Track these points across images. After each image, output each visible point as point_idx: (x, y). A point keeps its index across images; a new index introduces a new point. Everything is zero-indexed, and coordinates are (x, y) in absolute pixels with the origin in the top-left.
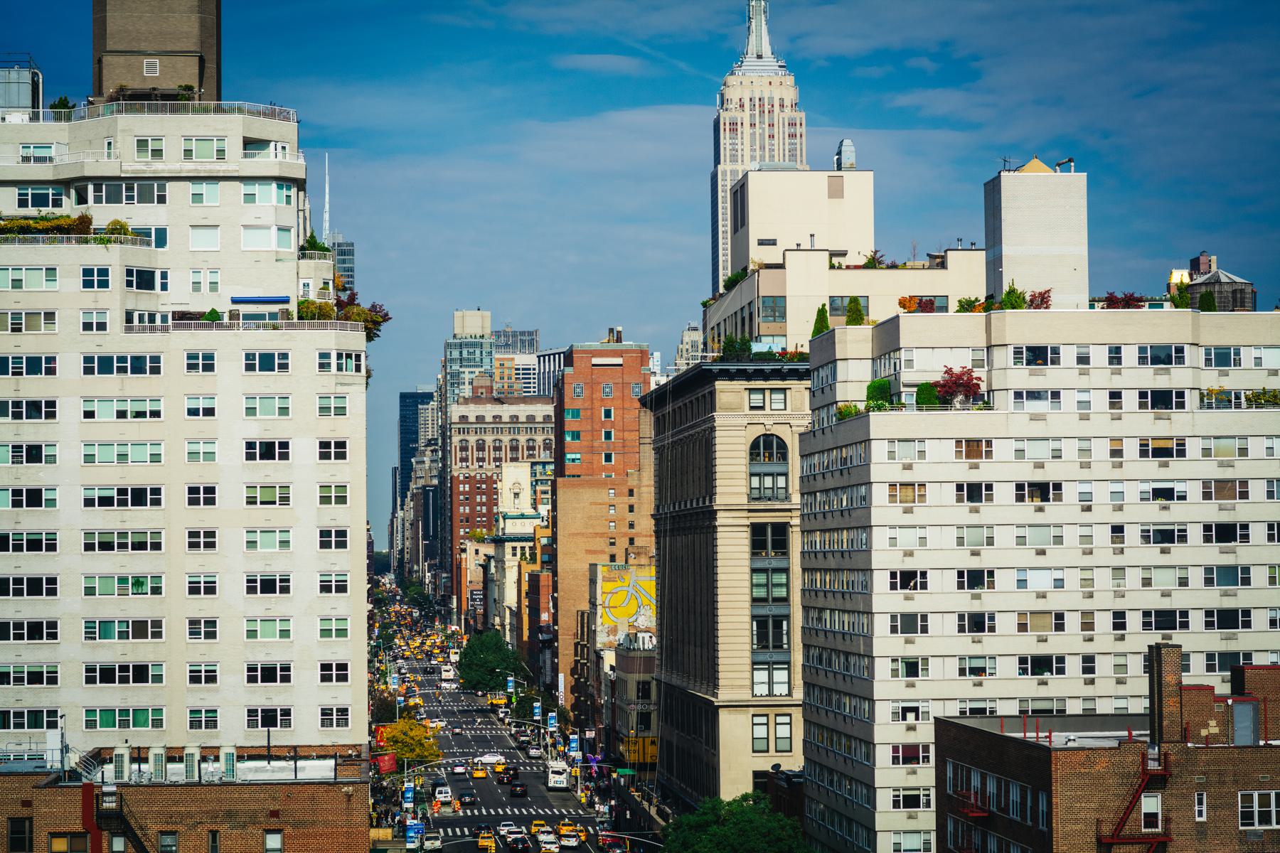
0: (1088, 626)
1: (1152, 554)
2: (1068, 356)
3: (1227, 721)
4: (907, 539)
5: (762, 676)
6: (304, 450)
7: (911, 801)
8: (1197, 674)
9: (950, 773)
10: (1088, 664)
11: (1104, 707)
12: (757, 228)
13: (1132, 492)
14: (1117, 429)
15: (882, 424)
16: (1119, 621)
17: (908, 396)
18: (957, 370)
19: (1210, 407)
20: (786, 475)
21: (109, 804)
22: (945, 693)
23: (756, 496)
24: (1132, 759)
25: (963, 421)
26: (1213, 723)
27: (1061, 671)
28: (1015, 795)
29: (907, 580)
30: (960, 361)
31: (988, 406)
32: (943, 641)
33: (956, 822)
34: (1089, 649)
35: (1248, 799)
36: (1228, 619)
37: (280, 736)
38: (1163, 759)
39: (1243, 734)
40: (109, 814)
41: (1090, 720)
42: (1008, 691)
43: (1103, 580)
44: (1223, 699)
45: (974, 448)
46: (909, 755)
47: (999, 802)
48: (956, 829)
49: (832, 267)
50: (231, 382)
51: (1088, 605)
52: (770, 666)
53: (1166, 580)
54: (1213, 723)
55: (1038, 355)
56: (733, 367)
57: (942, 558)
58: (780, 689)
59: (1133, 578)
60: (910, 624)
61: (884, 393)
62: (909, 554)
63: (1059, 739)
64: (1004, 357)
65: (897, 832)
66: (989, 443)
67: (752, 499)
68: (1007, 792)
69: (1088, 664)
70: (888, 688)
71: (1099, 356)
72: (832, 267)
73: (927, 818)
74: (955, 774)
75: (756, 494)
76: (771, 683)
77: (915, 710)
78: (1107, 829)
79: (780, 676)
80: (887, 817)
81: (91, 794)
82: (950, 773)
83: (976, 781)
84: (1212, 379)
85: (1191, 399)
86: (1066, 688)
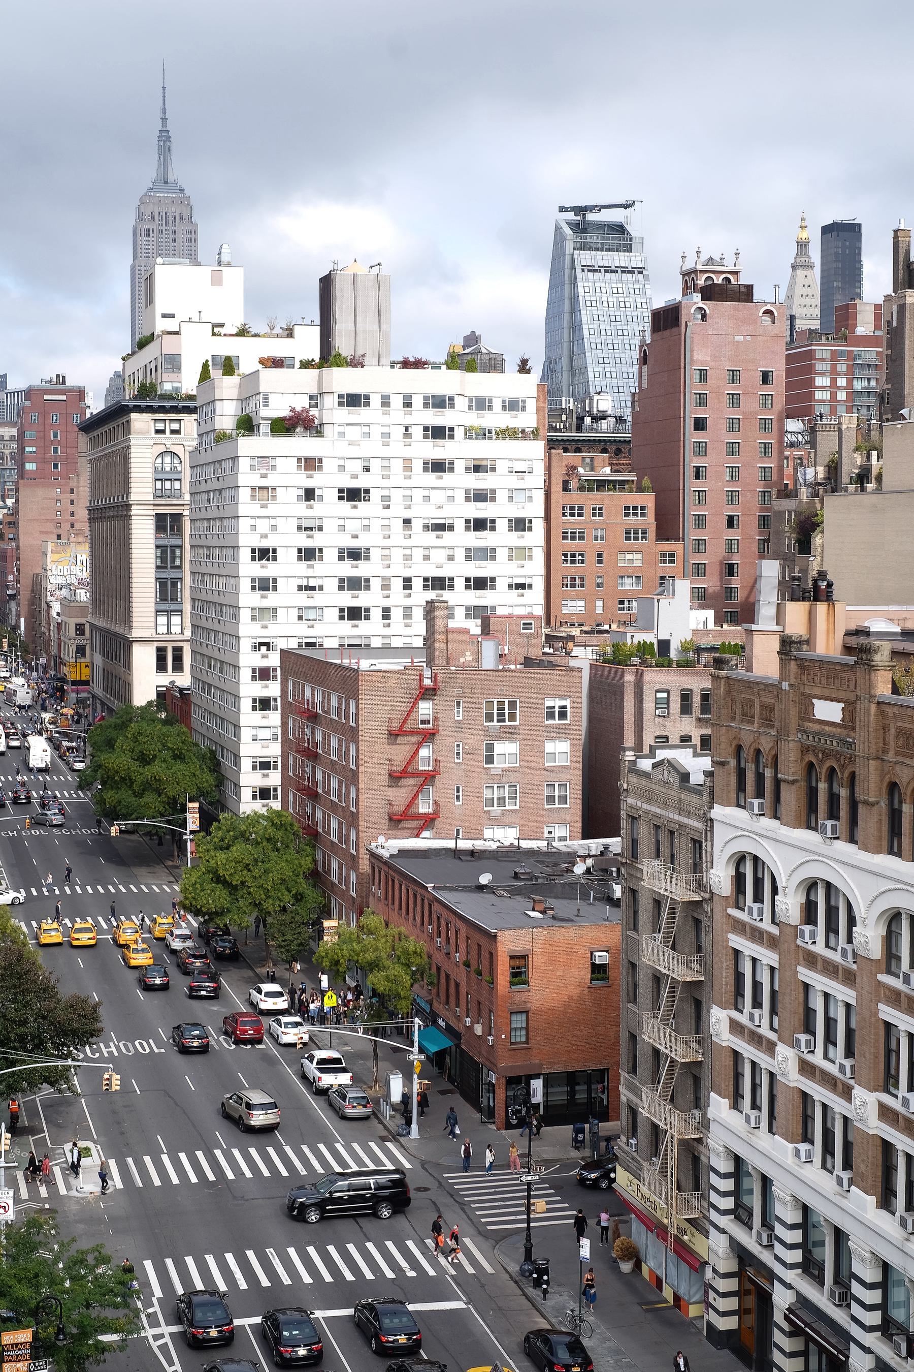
0: (386, 587)
1: (431, 538)
2: (376, 401)
3: (478, 653)
4: (263, 526)
5: (162, 620)
7: (264, 704)
8: (459, 621)
9: (290, 687)
10: (386, 613)
11: (396, 643)
12: (161, 304)
13: (418, 495)
14: (408, 453)
15: (247, 446)
16: (407, 583)
17: (265, 427)
18: (299, 409)
19: (471, 438)
20: (180, 480)
22: (288, 633)
23: (159, 494)
24: (413, 677)
25: (301, 444)
26: (468, 654)
27: (368, 618)
28: (334, 702)
29: (264, 554)
31: (319, 433)
32: (286, 596)
33: (294, 720)
34: (386, 603)
36: (480, 583)
38: (434, 678)
39: (489, 661)
41: (387, 650)
42: (331, 632)
43: (397, 555)
44: (475, 637)
45: (310, 464)
46: (263, 674)
47: (323, 707)
48: (294, 725)
49: (214, 334)
51: (387, 573)
52: (169, 613)
53: (438, 556)
54: (468, 654)
55: (354, 400)
56: (143, 404)
57: (287, 541)
58: (176, 629)
59: (418, 554)
60: (264, 585)
61: (247, 425)
62: (264, 536)
64: (330, 401)
65: (254, 727)
66: (320, 461)
67: (156, 496)
68: (329, 700)
69: (386, 613)
70: (249, 629)
71: (397, 401)
72: (214, 334)
73: (274, 718)
74: (294, 688)
75: (159, 493)
76: (169, 625)
77: (267, 645)
78: (396, 725)
79: (176, 620)
80: (248, 717)
82: (290, 687)
83: (308, 693)
85: (459, 433)
86: (370, 629)
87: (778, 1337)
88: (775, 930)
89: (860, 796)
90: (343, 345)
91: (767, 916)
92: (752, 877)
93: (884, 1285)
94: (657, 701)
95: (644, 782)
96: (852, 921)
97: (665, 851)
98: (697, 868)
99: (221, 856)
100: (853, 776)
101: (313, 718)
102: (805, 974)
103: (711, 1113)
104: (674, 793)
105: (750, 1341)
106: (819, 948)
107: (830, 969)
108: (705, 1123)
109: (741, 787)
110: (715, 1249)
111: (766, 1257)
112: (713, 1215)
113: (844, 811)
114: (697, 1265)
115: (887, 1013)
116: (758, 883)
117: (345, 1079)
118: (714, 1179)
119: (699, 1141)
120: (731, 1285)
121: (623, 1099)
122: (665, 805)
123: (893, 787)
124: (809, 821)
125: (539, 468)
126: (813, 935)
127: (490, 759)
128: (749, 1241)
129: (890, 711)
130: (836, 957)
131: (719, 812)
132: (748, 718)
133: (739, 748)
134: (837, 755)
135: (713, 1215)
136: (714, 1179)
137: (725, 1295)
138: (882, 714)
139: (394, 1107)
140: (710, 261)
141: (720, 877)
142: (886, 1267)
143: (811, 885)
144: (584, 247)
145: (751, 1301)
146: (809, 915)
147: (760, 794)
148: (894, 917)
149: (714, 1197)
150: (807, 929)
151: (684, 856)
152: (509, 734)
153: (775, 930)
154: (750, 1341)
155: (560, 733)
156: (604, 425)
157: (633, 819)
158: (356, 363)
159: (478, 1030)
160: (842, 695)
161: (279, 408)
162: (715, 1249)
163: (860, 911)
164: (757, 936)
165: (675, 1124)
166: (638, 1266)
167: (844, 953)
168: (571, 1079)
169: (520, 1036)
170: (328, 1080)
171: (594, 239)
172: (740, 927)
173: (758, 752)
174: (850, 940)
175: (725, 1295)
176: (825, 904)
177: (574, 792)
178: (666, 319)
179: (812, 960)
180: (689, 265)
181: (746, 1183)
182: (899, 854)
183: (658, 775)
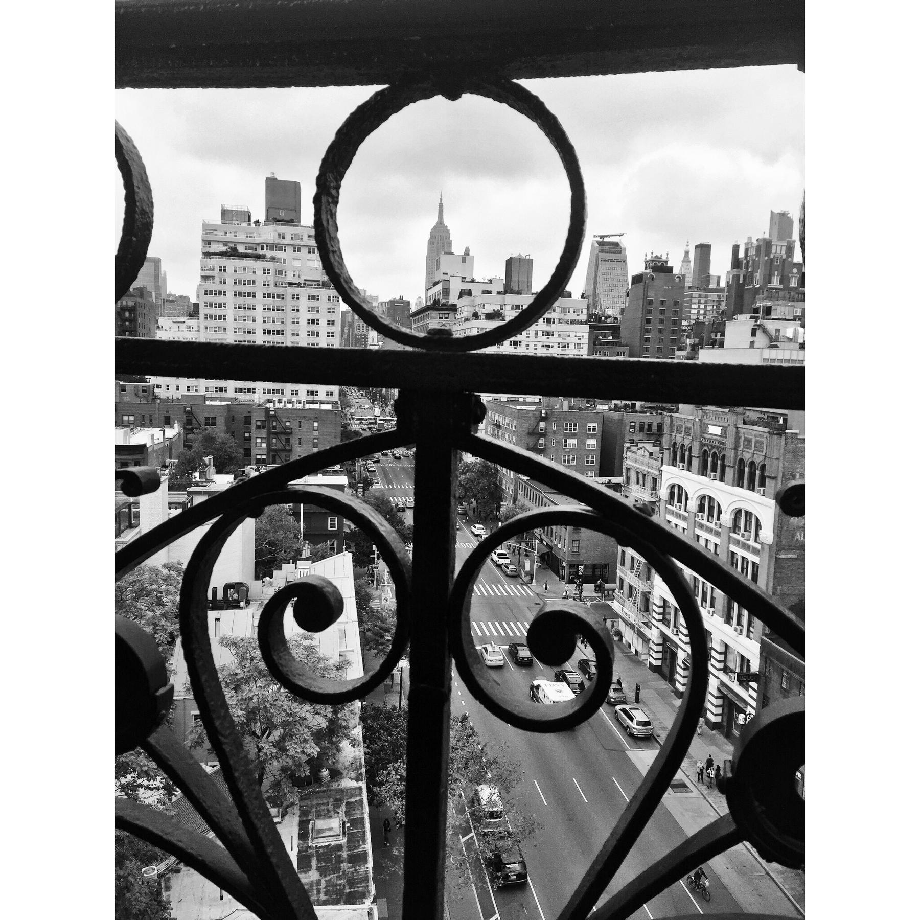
6: (323, 322)
12: (443, 269)
13: (539, 345)
17: (483, 317)
21: (272, 413)
30: (497, 308)
35: (566, 425)
37: (316, 398)
38: (546, 413)
40: (272, 416)
50: (303, 303)
63: (519, 407)
64: (508, 307)
81: (267, 410)
83: (497, 417)
84: (562, 316)
85: (556, 321)
87: (679, 670)
88: (686, 514)
89: (726, 463)
90: (515, 287)
91: (683, 508)
92: (677, 494)
93: (725, 653)
94: (631, 427)
95: (633, 455)
96: (720, 512)
97: (641, 482)
98: (654, 489)
99: (462, 477)
100: (724, 455)
101: (499, 427)
102: (698, 531)
103: (655, 583)
104: (647, 459)
105: (666, 670)
106: (705, 522)
107: (710, 530)
108: (652, 586)
109: (675, 459)
110: (653, 634)
111: (675, 639)
112: (654, 621)
113: (718, 470)
114: (646, 640)
115: (733, 548)
116: (680, 496)
117: (507, 561)
118: (655, 608)
119: (649, 593)
120: (660, 648)
121: (618, 575)
122: (642, 464)
123: (741, 460)
124: (703, 472)
125: (586, 336)
126: (702, 517)
127: (565, 445)
128: (669, 632)
129: (742, 431)
130: (712, 526)
131: (665, 468)
132: (679, 431)
133: (675, 443)
134: (718, 448)
135: (654, 621)
136: (655, 608)
137: (657, 652)
138: (737, 432)
139: (527, 574)
140: (656, 257)
141: (664, 493)
142: (726, 646)
143: (703, 498)
144: (602, 251)
145: (668, 656)
146: (701, 508)
147: (682, 461)
148: (738, 512)
149: (654, 615)
150: (700, 514)
151: (649, 483)
152: (573, 436)
153: (686, 514)
154: (666, 670)
155: (593, 436)
156: (609, 320)
157: (628, 469)
158: (519, 293)
159: (559, 546)
160: (721, 424)
161: (489, 309)
162: (653, 634)
163: (723, 508)
164: (679, 516)
165: (640, 586)
166: (621, 639)
167: (716, 524)
168: (594, 567)
169: (576, 550)
170: (502, 561)
171: (606, 248)
172: (671, 513)
173: (683, 445)
174: (718, 519)
175: (657, 652)
176: (708, 506)
177: (596, 459)
178: (637, 279)
179: (701, 526)
180: (649, 258)
181: (668, 610)
182: (742, 487)
183: (639, 452)
